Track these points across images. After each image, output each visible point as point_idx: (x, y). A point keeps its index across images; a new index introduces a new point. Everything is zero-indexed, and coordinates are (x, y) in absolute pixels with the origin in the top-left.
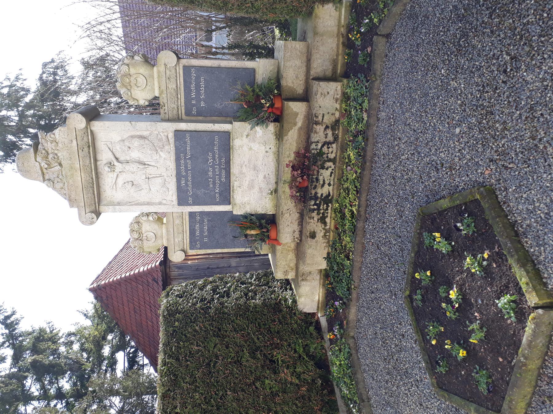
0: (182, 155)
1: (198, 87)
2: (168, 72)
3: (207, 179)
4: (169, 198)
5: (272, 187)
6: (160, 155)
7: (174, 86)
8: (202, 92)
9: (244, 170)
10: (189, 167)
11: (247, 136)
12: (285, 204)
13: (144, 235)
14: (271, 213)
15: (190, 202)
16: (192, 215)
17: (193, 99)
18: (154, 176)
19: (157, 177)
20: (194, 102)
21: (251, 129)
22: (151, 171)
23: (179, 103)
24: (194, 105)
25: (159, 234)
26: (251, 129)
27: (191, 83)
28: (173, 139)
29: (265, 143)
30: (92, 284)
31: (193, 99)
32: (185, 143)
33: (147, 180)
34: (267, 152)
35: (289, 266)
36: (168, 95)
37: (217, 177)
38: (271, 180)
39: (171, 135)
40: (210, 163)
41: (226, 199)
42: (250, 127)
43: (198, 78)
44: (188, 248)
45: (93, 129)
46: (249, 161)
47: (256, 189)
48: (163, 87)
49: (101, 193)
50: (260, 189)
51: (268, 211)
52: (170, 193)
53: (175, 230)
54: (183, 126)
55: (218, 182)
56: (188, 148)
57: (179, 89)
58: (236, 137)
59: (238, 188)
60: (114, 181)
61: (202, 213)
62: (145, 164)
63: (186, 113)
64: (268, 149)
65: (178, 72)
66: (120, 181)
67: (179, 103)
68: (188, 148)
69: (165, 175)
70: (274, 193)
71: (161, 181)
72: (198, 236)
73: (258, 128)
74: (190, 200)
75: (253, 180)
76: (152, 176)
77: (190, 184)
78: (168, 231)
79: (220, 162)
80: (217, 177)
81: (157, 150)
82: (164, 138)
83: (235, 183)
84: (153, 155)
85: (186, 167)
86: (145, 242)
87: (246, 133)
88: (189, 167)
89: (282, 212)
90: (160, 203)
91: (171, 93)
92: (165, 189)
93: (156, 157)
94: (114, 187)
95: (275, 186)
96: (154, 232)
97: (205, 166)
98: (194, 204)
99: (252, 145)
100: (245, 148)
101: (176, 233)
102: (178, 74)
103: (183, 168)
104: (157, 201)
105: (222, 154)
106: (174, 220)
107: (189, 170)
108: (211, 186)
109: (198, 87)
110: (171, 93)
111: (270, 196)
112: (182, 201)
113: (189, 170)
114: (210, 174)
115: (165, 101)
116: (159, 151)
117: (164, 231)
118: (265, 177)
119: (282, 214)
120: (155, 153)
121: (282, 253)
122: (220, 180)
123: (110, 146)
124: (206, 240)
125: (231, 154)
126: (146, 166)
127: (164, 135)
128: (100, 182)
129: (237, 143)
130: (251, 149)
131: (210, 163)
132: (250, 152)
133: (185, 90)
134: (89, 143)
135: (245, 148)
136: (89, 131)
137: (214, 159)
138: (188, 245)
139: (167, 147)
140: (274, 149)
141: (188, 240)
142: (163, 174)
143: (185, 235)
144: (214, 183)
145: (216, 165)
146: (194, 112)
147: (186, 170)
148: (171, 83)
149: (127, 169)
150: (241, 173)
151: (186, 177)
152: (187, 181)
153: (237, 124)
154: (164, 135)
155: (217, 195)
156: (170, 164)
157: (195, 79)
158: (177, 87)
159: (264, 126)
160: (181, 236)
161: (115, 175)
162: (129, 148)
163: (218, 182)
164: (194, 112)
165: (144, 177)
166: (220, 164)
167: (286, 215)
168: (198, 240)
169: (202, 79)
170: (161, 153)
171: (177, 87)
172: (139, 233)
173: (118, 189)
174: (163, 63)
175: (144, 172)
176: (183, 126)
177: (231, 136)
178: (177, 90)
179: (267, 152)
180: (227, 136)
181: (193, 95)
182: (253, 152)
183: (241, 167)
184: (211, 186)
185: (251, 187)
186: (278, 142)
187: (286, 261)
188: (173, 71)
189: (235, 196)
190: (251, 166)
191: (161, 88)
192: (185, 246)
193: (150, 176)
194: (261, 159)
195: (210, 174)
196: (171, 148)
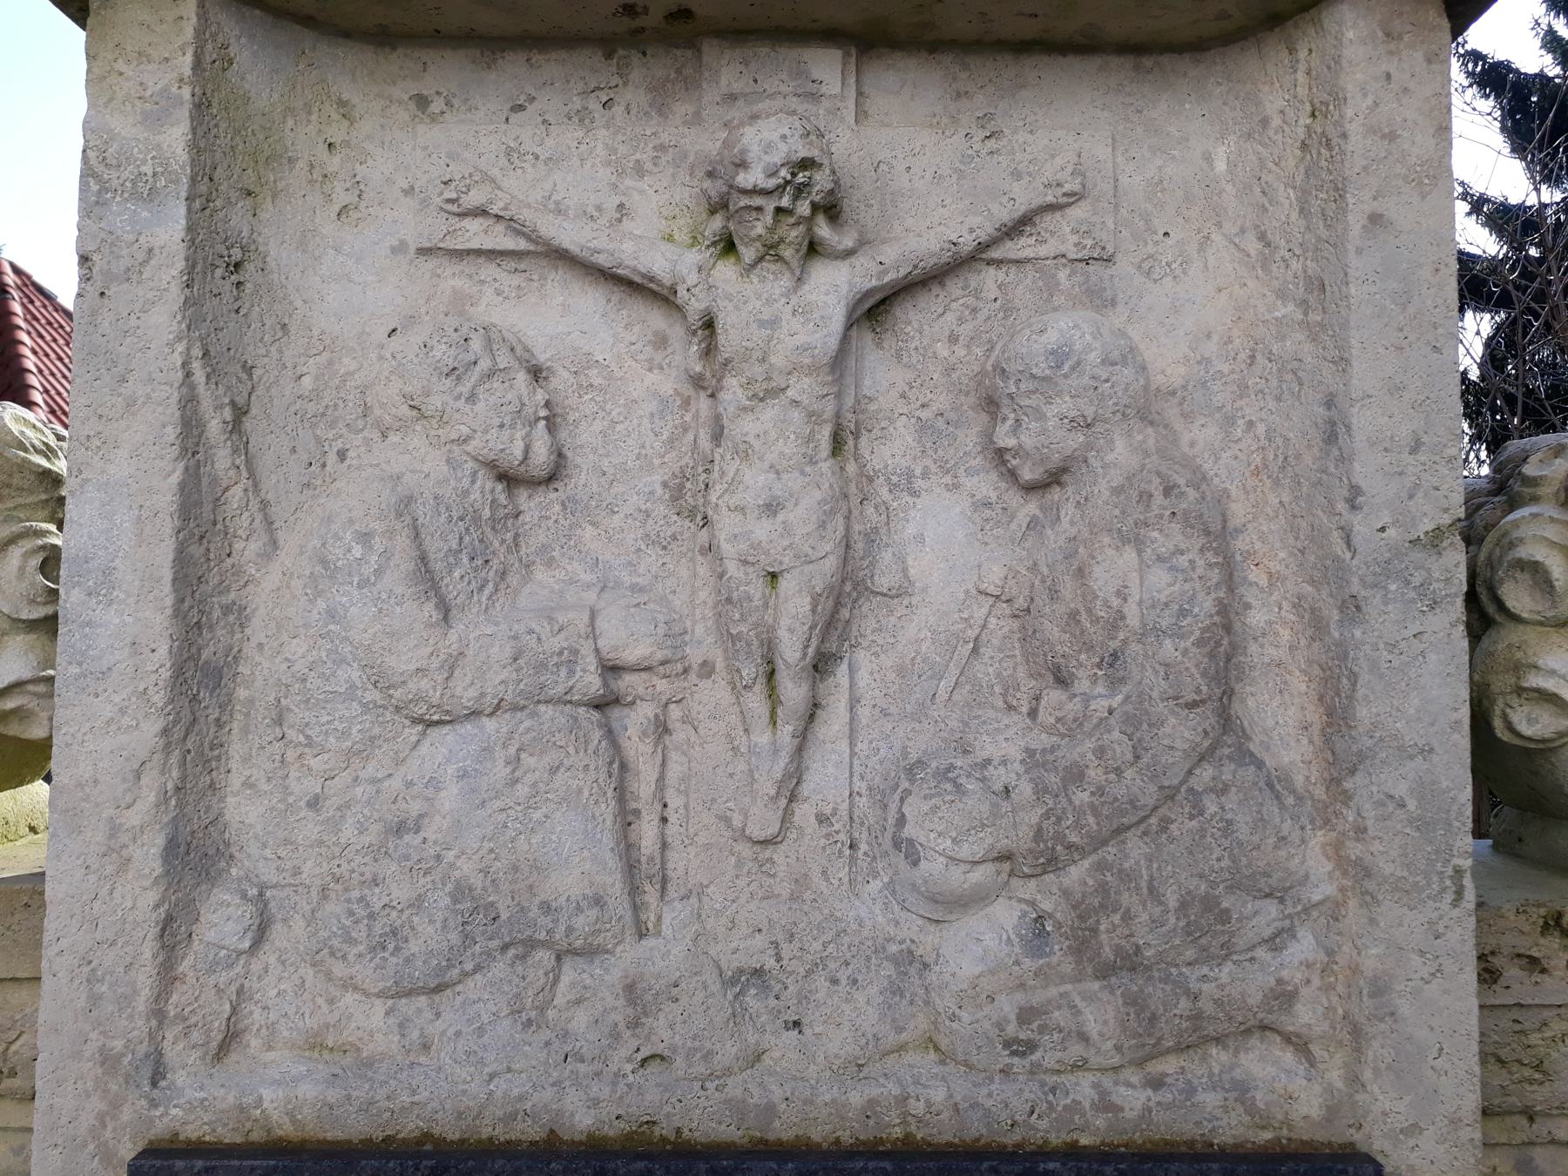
4: (283, 995)
18: (643, 786)
19: (627, 818)
22: (715, 746)
28: (1231, 1128)
30: (17, 270)
33: (592, 683)
49: (395, 61)
52: (369, 1022)
60: (570, 236)
62: (821, 665)
66: (564, 321)
69: (665, 954)
71: (566, 884)
76: (637, 748)
81: (1052, 864)
82: (1243, 982)
84: (976, 802)
90: (194, 856)
92: (429, 937)
93: (949, 839)
94: (475, 234)
104: (244, 810)
116: (1046, 895)
120: (1021, 839)
123: (1059, 236)
126: (793, 692)
128: (552, 65)
139: (1099, 1014)
142: (673, 917)
149: (746, 427)
154: (1284, 996)
156: (837, 1043)
161: (658, 262)
165: (629, 637)
170: (1006, 915)
173: (454, 278)
175: (703, 644)
193: (634, 722)
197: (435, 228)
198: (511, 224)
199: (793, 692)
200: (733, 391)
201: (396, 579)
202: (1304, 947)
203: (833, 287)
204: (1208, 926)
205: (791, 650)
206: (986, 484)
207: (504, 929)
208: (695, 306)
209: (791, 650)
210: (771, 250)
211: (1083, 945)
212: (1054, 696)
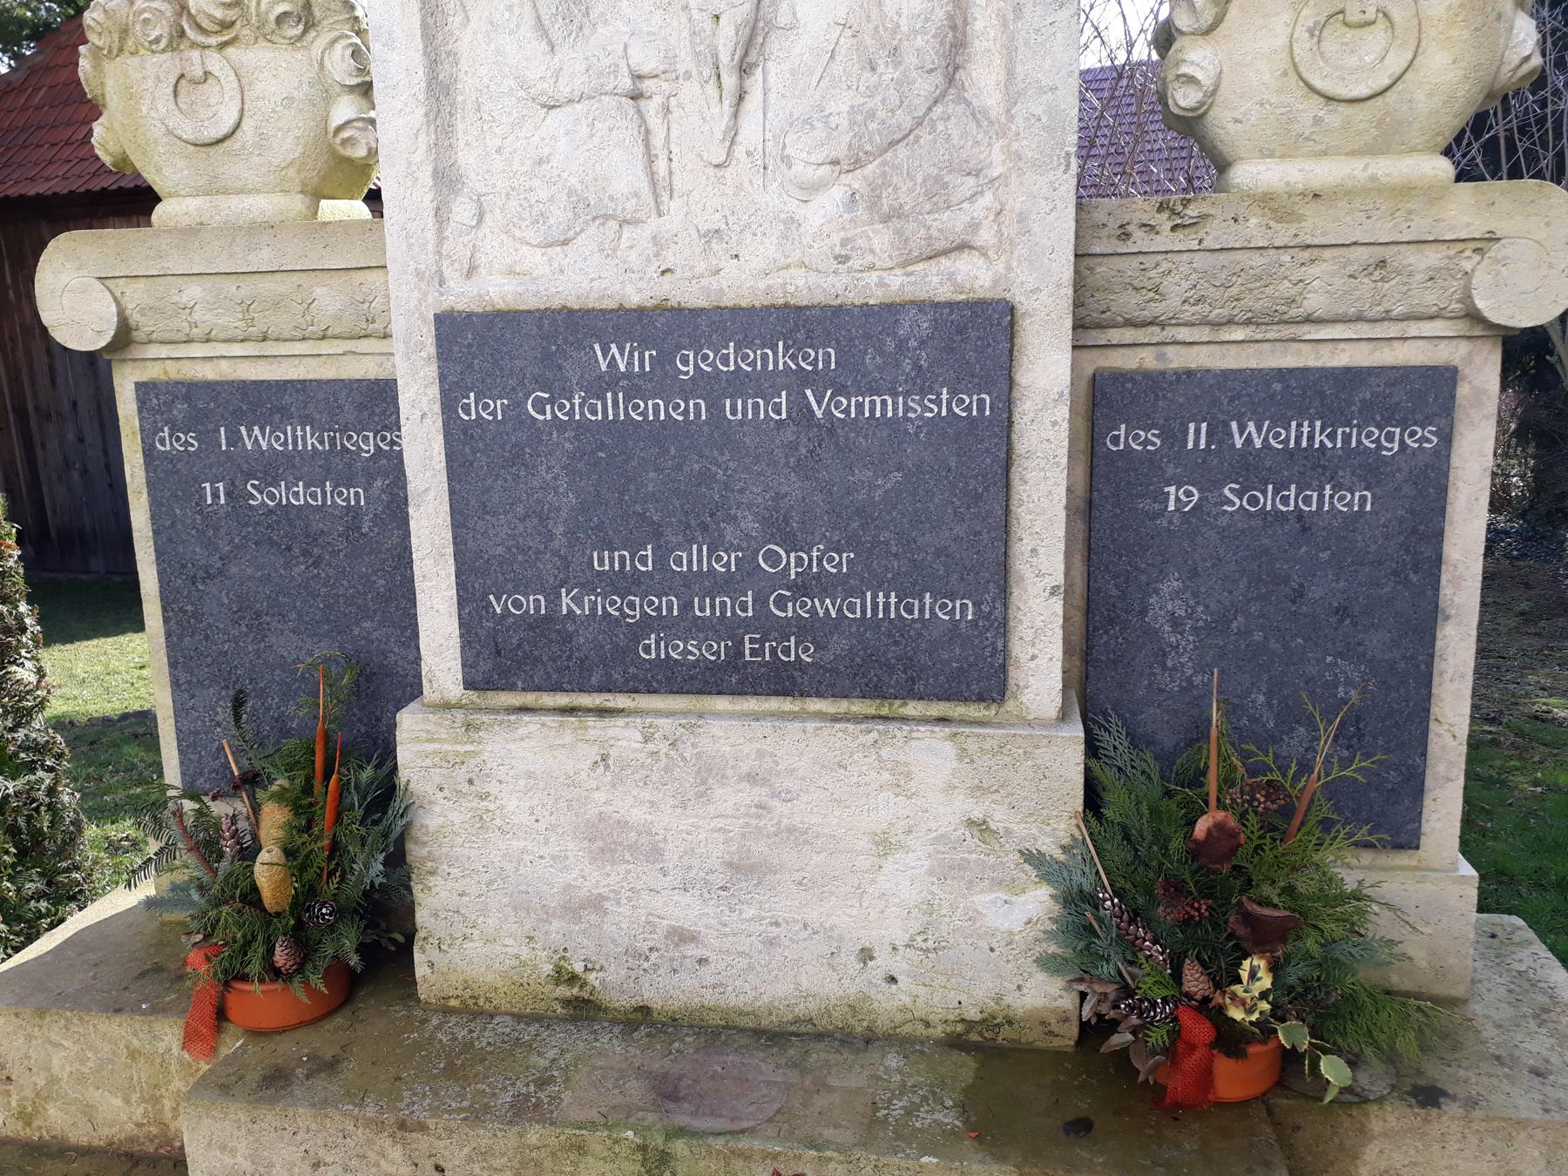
0: (825, 357)
1: (1313, 467)
2: (1432, 257)
4: (495, 249)
5: (614, 983)
6: (815, 188)
7: (1315, 303)
8: (1268, 501)
9: (731, 798)
10: (736, 410)
11: (980, 827)
12: (485, 1154)
13: (215, 62)
14: (421, 970)
15: (472, 408)
17: (1218, 432)
18: (658, 141)
19: (650, 159)
20: (1197, 436)
21: (1033, 858)
22: (696, 113)
23: (1183, 334)
24: (1173, 436)
25: (232, 169)
26: (1033, 858)
28: (944, 293)
29: (927, 945)
31: (1218, 432)
32: (922, 384)
33: (626, 83)
34: (866, 955)
35: (43, 1097)
36: (1257, 260)
37: (670, 605)
38: (664, 980)
39: (972, 276)
40: (773, 558)
41: (509, 662)
42: (1049, 846)
43: (1370, 469)
46: (795, 834)
47: (592, 878)
48: (1317, 225)
50: (596, 903)
51: (435, 955)
52: (534, 259)
53: (267, 285)
54: (1047, 373)
55: (636, 608)
56: (885, 406)
57: (1288, 331)
58: (972, 745)
59: (594, 753)
62: (744, 69)
63: (1120, 377)
64: (883, 962)
65: (1414, 329)
67: (1183, 334)
68: (885, 406)
70: (564, 991)
71: (620, 186)
72: (235, 439)
73: (1034, 905)
75: (655, 853)
76: (654, 121)
77: (610, 407)
78: (257, 229)
79: (783, 630)
80: (670, 605)
81: (857, 164)
82: (953, 222)
83: (637, 731)
84: (820, 133)
85: (739, 384)
86: (163, 66)
87: (999, 817)
88: (736, 410)
89: (422, 1127)
90: (446, 180)
91: (1266, 277)
92: (559, 216)
93: (807, 156)
95: (621, 1000)
97: (750, 524)
98: (462, 442)
99: (916, 859)
100: (886, 810)
101: (247, 288)
102: (1393, 330)
104: (466, 158)
105: (839, 645)
106: (337, 280)
107: (715, 407)
108: (604, 562)
109: (1313, 467)
110: (1266, 277)
111: (548, 968)
112: (476, 345)
113: (715, 407)
114: (692, 559)
115: (1214, 234)
116: (855, 181)
117: (262, 205)
118: (681, 937)
119: (402, 1126)
120: (840, 151)
121: (133, 1054)
125: (842, 706)
126: (730, 81)
127: (974, 226)
130: (885, 845)
131: (773, 558)
132: (864, 843)
133: (1282, 374)
135: (886, 810)
137: (802, 588)
138: (173, 372)
139: (881, 240)
140: (889, 1005)
141: (208, 373)
142: (674, 206)
143: (237, 350)
145: (761, 601)
146: (1124, 439)
147: (711, 387)
148: (1338, 282)
150: (708, 774)
151: (662, 382)
152: (635, 387)
153: (1066, 757)
154: (974, 226)
155: (535, 603)
157: (1361, 450)
158: (1309, 320)
159: (1053, 949)
160: (231, 321)
163: (636, 608)
165: (648, 62)
166: (766, 627)
167: (396, 1153)
169: (1357, 499)
170: (838, 193)
171: (1309, 320)
172: (226, 25)
174: (1501, 227)
175: (686, 63)
176: (1047, 373)
177: (974, 711)
178: (1286, 319)
179: (866, 955)
180: (971, 676)
181: (1249, 435)
182: (863, 862)
183: (752, 778)
184: (604, 562)
185: (606, 838)
186: (938, 1032)
187: (80, 1079)
188: (1430, 299)
189: (530, 724)
190: (759, 848)
192: (164, 351)
193: (651, 107)
194: (812, 916)
195: (692, 559)
196: (879, 278)
201: (527, 29)
202: (987, 199)
204: (937, 192)
207: (595, 211)
211: (873, 204)
212: (867, 75)
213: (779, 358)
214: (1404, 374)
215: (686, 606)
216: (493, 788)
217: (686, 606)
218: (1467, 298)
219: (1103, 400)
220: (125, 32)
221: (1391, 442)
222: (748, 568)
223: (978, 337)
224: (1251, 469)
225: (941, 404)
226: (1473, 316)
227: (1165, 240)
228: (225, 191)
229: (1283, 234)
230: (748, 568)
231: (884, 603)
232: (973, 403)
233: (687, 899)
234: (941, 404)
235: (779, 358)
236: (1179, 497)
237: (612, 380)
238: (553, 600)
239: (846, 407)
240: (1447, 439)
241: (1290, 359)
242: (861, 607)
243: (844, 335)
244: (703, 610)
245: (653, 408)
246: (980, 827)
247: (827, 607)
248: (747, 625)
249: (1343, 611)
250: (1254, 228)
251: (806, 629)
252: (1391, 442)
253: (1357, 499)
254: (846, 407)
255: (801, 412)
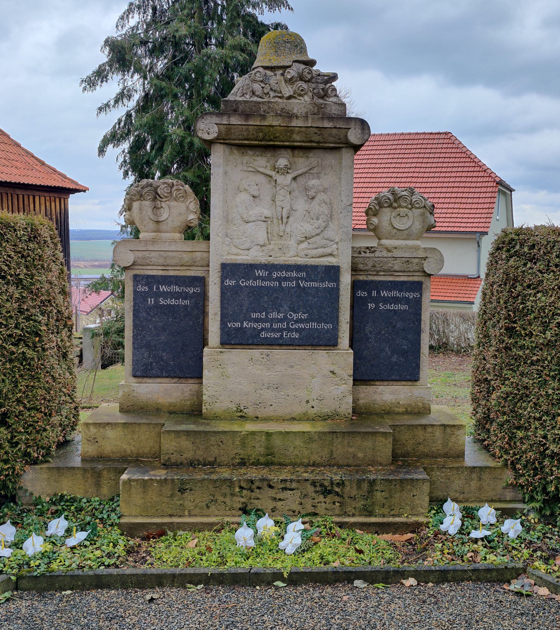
0: (304, 274)
1: (396, 300)
2: (416, 260)
3: (265, 310)
7: (396, 268)
8: (388, 307)
10: (284, 284)
11: (333, 372)
15: (228, 282)
16: (201, 282)
17: (378, 293)
20: (374, 293)
23: (371, 273)
24: (370, 293)
27: (400, 291)
31: (378, 293)
32: (323, 281)
34: (308, 402)
36: (385, 259)
37: (268, 325)
39: (332, 261)
40: (291, 315)
43: (407, 301)
44: (137, 272)
45: (344, 150)
48: (396, 254)
54: (346, 279)
55: (260, 326)
57: (392, 273)
60: (261, 170)
61: (204, 296)
62: (288, 218)
63: (360, 281)
64: (312, 403)
65: (415, 274)
72: (158, 288)
74: (230, 283)
77: (258, 283)
80: (268, 325)
85: (286, 279)
94: (250, 169)
96: (169, 221)
97: (286, 308)
98: (224, 290)
103: (284, 274)
107: (280, 284)
108: (254, 315)
109: (396, 300)
112: (228, 270)
113: (280, 284)
114: (273, 315)
122: (263, 329)
124: (151, 301)
129: (321, 357)
131: (291, 315)
133: (390, 282)
134: (325, 143)
136: (341, 146)
137: (297, 321)
144: (257, 320)
145: (288, 324)
146: (361, 294)
147: (278, 279)
148: (400, 264)
151: (269, 278)
152: (263, 279)
155: (238, 325)
157: (405, 297)
158: (395, 271)
160: (161, 261)
162: (313, 198)
163: (260, 326)
164: (361, 294)
168: (151, 288)
169: (406, 307)
171: (395, 271)
174: (428, 255)
176: (346, 279)
178: (390, 271)
179: (308, 402)
184: (254, 315)
188: (417, 268)
191: (394, 250)
195: (273, 315)
197: (245, 168)
198: (254, 168)
199: (285, 220)
200: (278, 188)
203: (289, 177)
205: (285, 216)
206: (306, 198)
208: (275, 178)
209: (285, 216)
210: (283, 173)
212: (312, 221)
213: (294, 274)
214: (414, 282)
215: (271, 325)
216: (225, 366)
217: (271, 325)
218: (423, 268)
219: (355, 286)
220: (141, 196)
221: (411, 295)
222: (285, 318)
223: (333, 272)
224: (386, 300)
225: (327, 284)
226: (424, 272)
227: (368, 255)
228: (160, 232)
229: (390, 255)
230: (285, 318)
231: (314, 325)
232: (332, 285)
233: (268, 391)
234: (327, 284)
235: (294, 274)
236: (371, 306)
237: (259, 277)
238: (242, 324)
239: (308, 284)
240: (421, 294)
241: (391, 279)
242: (308, 326)
243: (309, 271)
244: (275, 326)
245: (266, 283)
246: (333, 372)
247: (302, 326)
248: (284, 329)
249: (403, 330)
250: (385, 253)
251: (296, 330)
252: (411, 295)
253: (406, 307)
254: (308, 284)
255: (298, 285)
